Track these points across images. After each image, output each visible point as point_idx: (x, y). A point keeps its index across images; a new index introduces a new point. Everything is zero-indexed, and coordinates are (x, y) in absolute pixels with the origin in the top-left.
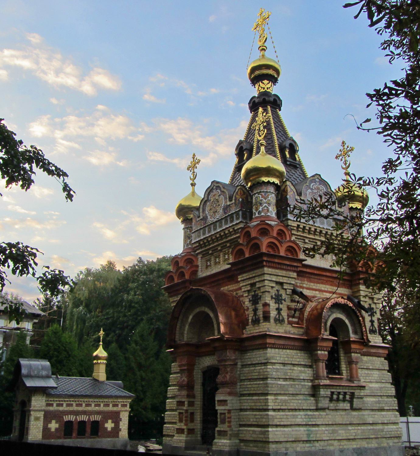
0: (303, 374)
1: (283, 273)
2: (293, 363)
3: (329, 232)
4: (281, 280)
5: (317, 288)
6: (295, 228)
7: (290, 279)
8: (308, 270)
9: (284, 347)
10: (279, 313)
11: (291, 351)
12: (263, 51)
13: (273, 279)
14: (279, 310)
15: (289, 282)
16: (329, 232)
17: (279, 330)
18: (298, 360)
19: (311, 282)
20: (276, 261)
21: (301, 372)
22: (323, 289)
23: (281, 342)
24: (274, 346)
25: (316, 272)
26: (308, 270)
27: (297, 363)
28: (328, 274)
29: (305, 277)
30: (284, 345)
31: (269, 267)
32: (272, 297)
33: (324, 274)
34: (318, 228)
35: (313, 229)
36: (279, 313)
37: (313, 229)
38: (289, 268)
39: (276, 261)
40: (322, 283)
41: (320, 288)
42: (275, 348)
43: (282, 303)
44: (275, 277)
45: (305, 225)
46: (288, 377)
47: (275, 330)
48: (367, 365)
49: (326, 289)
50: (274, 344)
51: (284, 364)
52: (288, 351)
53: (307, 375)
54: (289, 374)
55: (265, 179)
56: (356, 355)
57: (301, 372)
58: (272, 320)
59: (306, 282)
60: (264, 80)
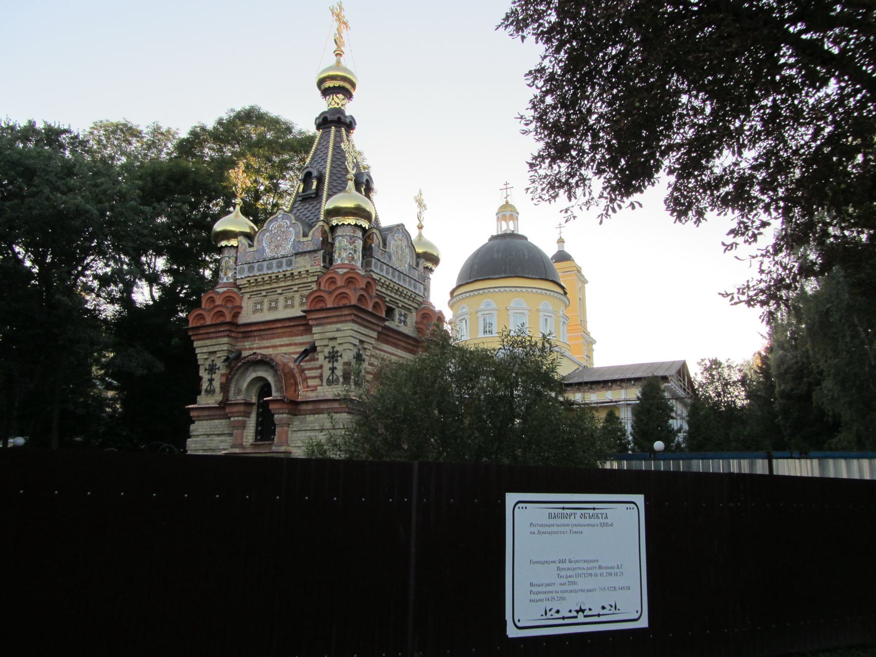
0: (223, 444)
1: (214, 341)
2: (216, 433)
3: (288, 273)
4: (212, 349)
5: (271, 344)
6: (247, 285)
7: (222, 346)
8: (254, 328)
9: (211, 418)
10: (211, 384)
11: (220, 421)
12: (338, 56)
13: (205, 351)
14: (211, 381)
15: (220, 349)
16: (288, 273)
17: (209, 402)
18: (222, 429)
19: (264, 339)
20: (201, 332)
21: (221, 441)
22: (278, 343)
23: (206, 413)
24: (200, 418)
25: (263, 328)
26: (254, 328)
27: (220, 432)
28: (279, 325)
29: (255, 336)
30: (209, 416)
31: (198, 340)
32: (206, 370)
33: (274, 326)
34: (272, 275)
35: (266, 278)
36: (211, 384)
37: (266, 278)
38: (218, 335)
39: (201, 332)
40: (278, 337)
41: (274, 344)
42: (203, 420)
43: (215, 373)
44: (205, 348)
45: (256, 278)
46: (206, 448)
47: (205, 402)
48: (311, 425)
49: (282, 343)
50: (198, 416)
51: (208, 435)
52: (216, 421)
53: (227, 444)
54: (208, 445)
55: (223, 243)
56: (281, 416)
57: (221, 441)
58: (203, 393)
59: (257, 342)
60: (339, 93)
